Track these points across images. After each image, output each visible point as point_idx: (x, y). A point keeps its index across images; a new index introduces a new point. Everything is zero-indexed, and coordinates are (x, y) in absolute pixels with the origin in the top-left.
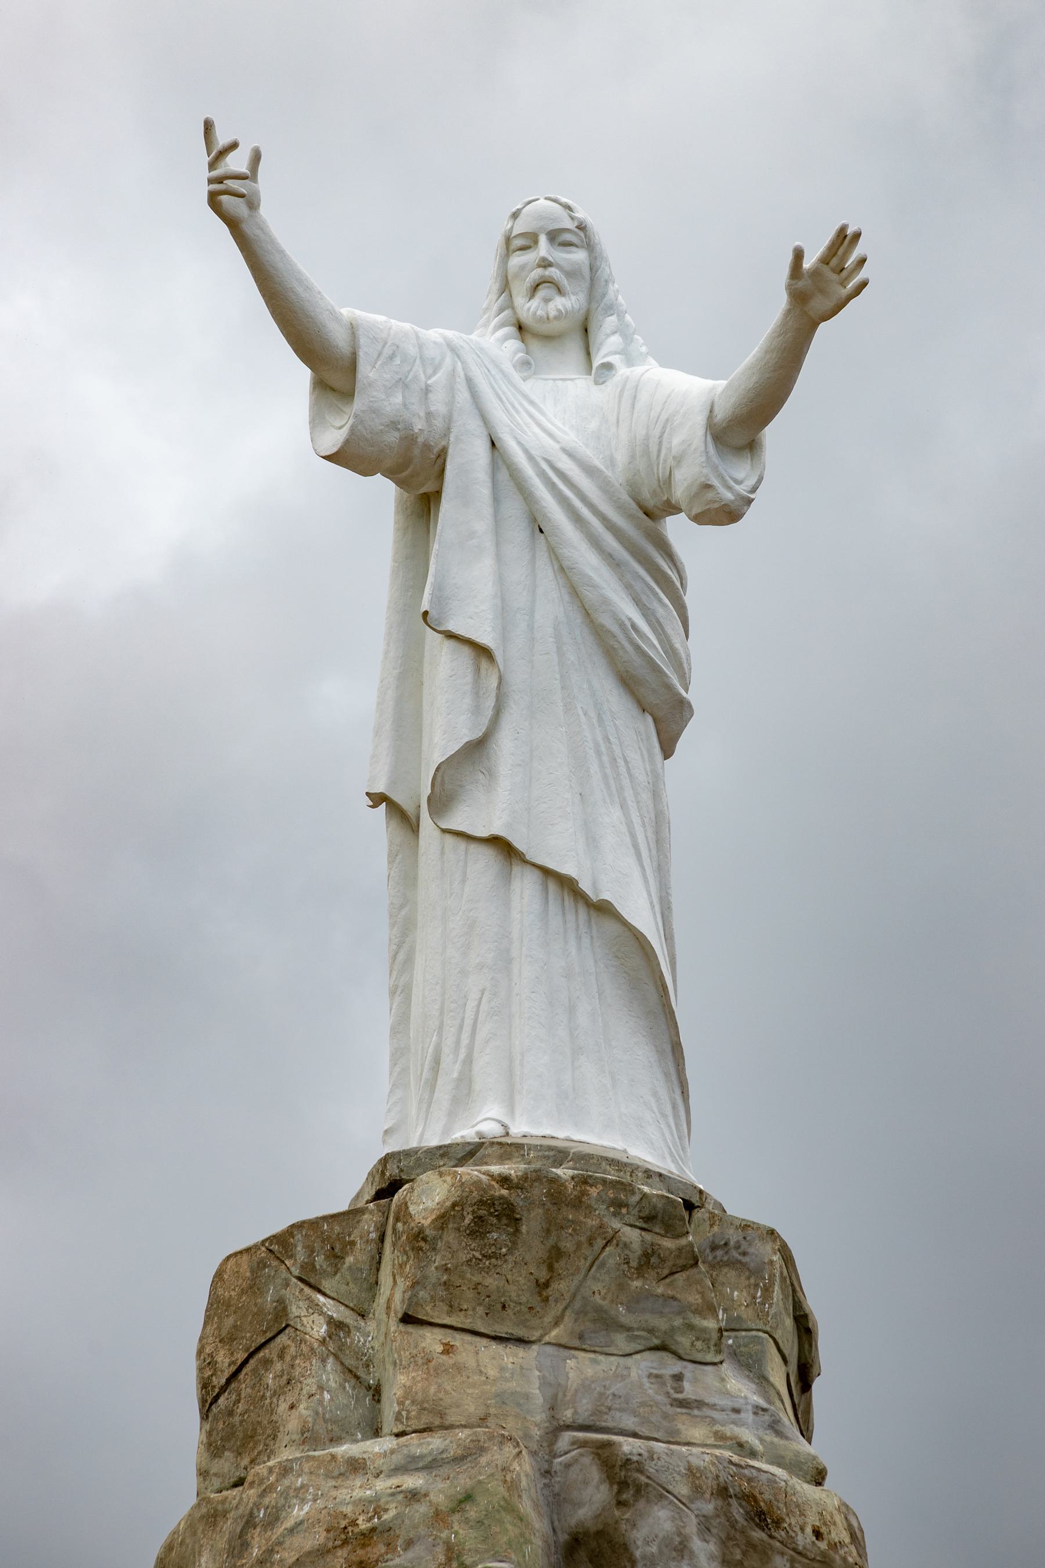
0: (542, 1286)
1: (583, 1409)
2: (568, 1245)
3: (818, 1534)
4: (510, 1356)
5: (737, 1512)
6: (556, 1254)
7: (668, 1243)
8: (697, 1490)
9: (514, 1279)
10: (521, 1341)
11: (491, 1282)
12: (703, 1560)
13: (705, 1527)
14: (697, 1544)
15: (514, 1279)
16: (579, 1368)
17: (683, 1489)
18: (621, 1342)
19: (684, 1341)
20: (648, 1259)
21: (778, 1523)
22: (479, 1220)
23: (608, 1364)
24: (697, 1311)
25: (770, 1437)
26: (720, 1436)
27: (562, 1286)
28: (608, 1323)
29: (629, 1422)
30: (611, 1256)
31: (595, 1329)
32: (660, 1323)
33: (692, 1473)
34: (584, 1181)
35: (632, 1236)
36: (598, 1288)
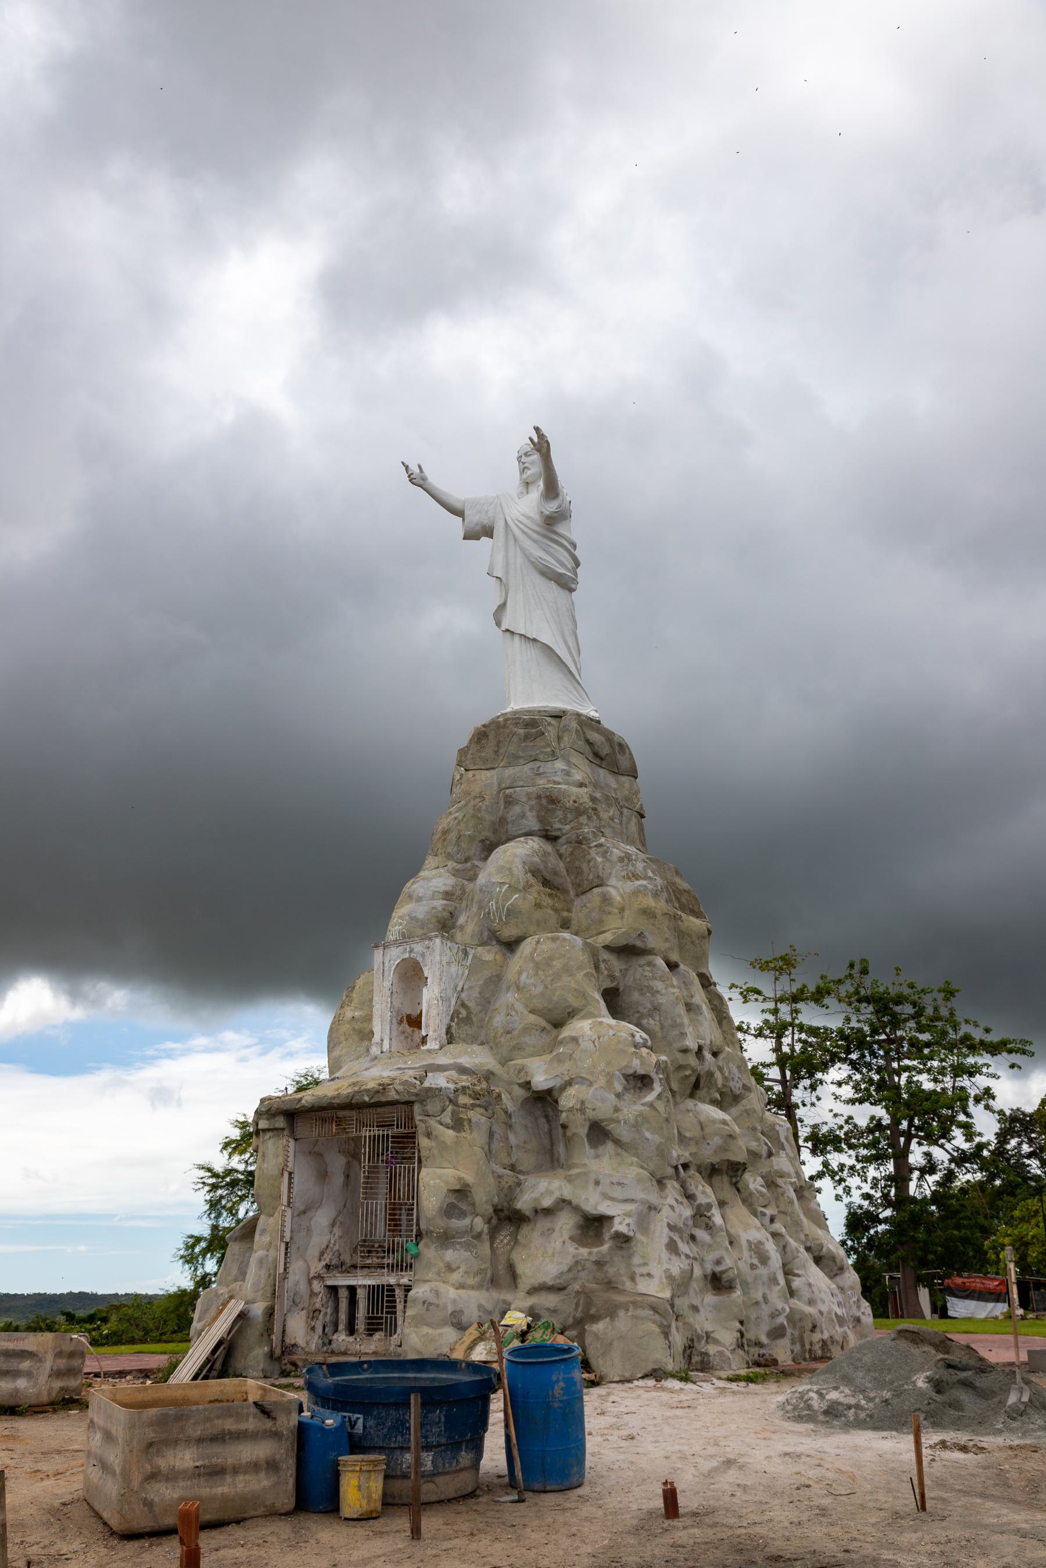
0: (496, 752)
1: (508, 783)
2: (502, 739)
3: (575, 802)
4: (489, 773)
5: (544, 801)
6: (499, 742)
7: (534, 731)
8: (529, 799)
9: (488, 752)
10: (493, 768)
11: (483, 754)
12: (530, 818)
13: (531, 809)
14: (528, 814)
15: (488, 752)
16: (509, 772)
17: (525, 799)
18: (522, 761)
19: (541, 757)
20: (527, 737)
21: (559, 802)
22: (479, 738)
23: (517, 769)
24: (544, 747)
25: (566, 777)
26: (549, 781)
27: (502, 751)
28: (516, 757)
29: (521, 783)
30: (515, 739)
31: (514, 760)
32: (533, 753)
33: (528, 794)
34: (506, 720)
35: (521, 732)
36: (512, 749)
